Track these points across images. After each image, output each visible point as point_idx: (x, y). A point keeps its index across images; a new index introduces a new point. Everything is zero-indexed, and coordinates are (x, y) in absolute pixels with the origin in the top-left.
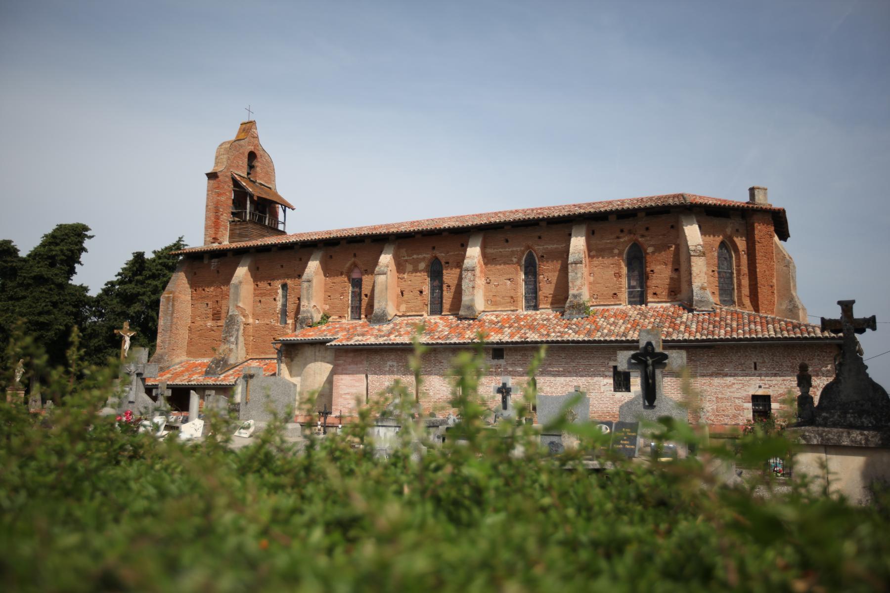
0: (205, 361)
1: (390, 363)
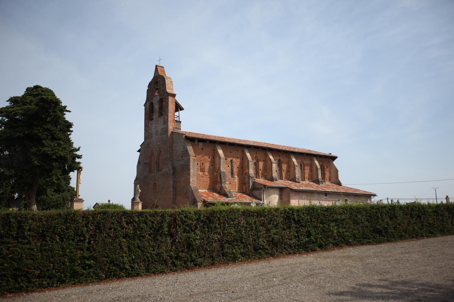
0: (338, 204)
1: (304, 196)
